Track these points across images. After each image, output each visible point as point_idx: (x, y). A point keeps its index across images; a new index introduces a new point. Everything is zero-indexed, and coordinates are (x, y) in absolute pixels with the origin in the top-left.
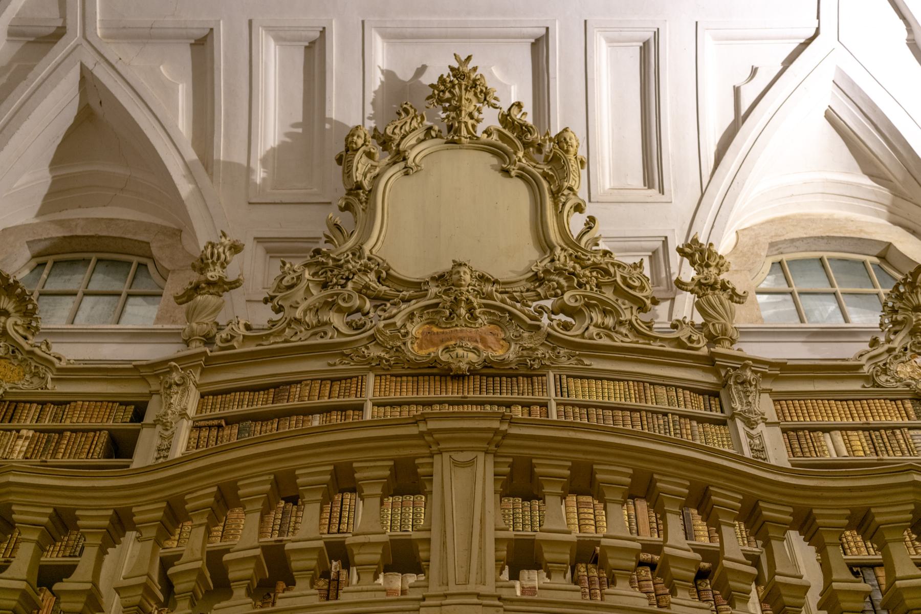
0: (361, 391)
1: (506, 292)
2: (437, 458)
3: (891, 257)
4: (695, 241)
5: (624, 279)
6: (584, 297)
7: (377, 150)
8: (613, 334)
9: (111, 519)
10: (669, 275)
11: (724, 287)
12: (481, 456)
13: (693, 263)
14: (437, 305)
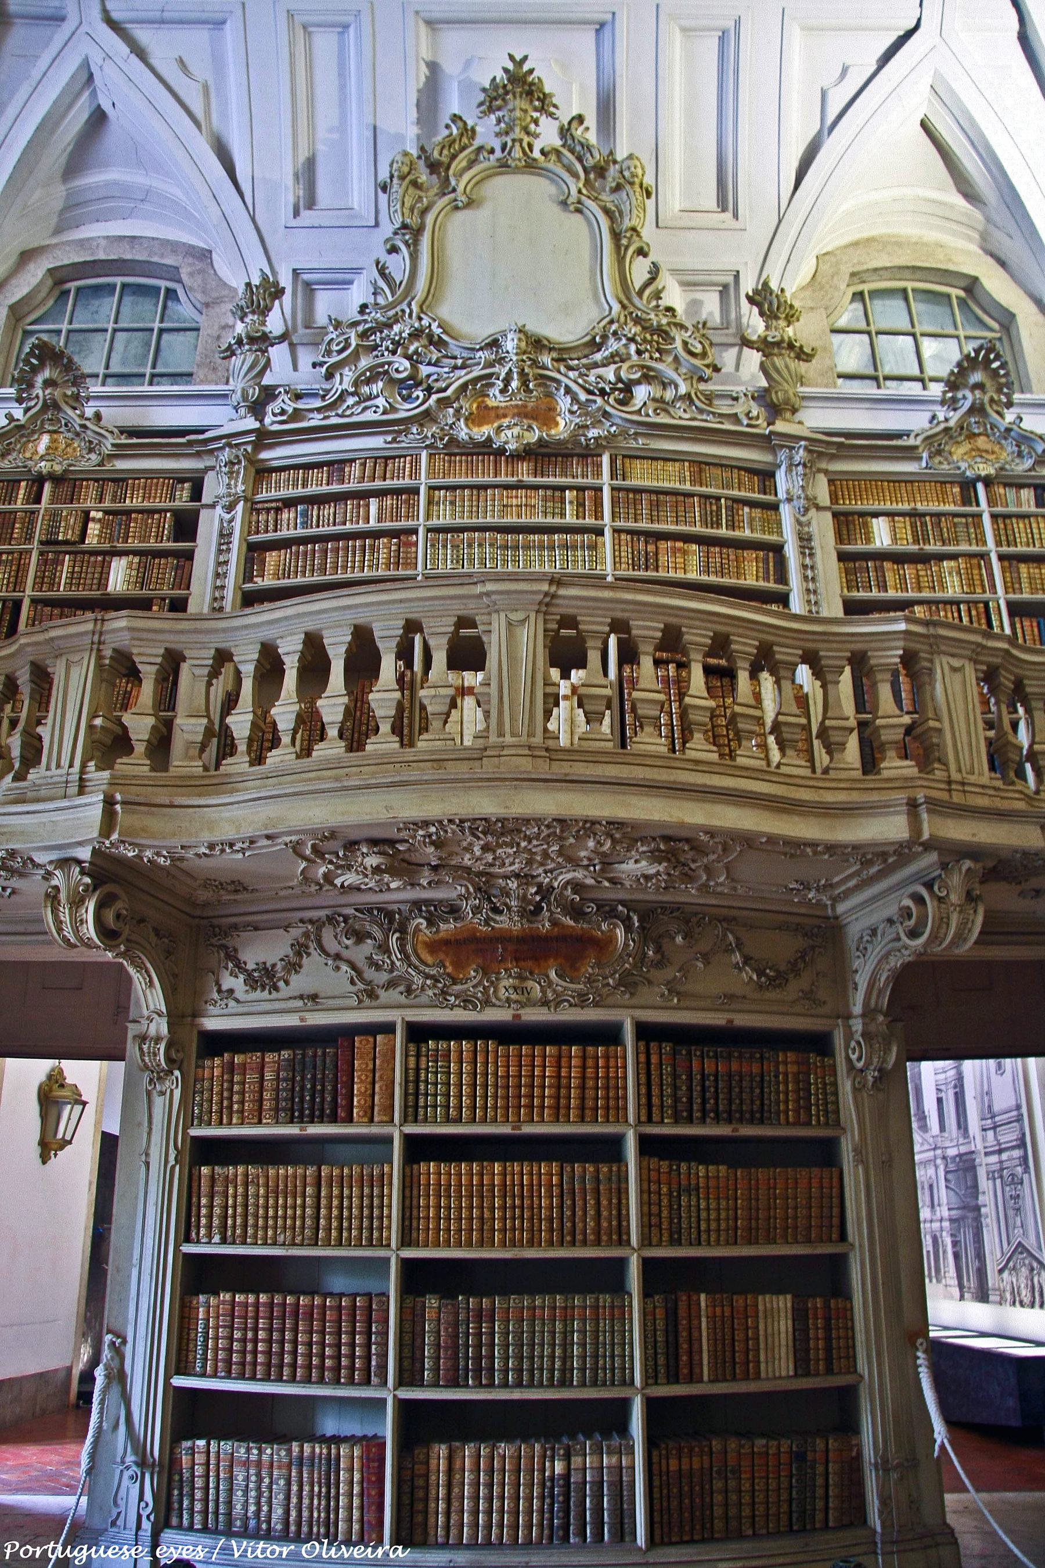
0: (415, 473)
1: (564, 360)
2: (495, 616)
3: (977, 291)
4: (766, 284)
5: (685, 343)
6: (643, 367)
7: (424, 177)
8: (671, 410)
9: (214, 658)
10: (739, 317)
11: (791, 346)
12: (533, 616)
13: (762, 314)
14: (490, 376)
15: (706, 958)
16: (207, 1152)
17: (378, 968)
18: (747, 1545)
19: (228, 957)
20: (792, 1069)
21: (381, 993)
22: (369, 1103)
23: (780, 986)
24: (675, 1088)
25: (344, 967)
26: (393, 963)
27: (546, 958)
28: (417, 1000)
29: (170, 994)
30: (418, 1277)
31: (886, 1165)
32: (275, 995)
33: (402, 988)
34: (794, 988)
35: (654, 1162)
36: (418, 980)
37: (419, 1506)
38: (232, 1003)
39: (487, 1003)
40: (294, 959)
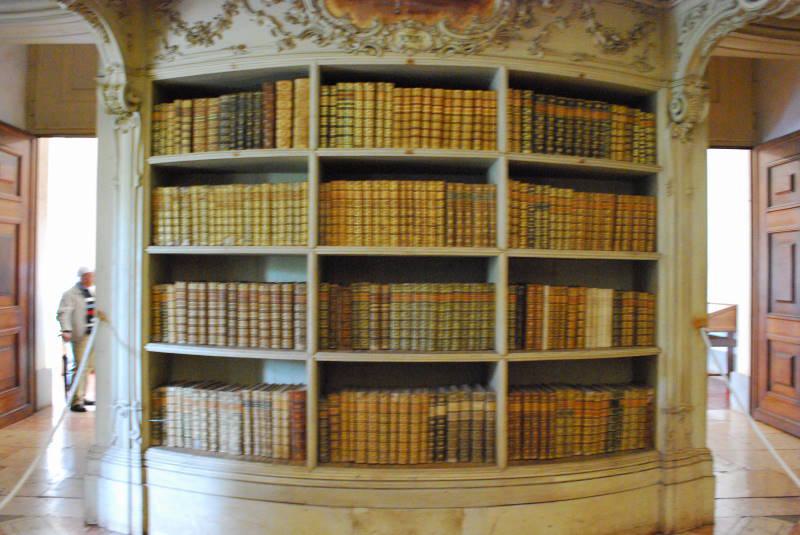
15: (566, 20)
16: (166, 176)
17: (294, 20)
18: (575, 465)
19: (173, 19)
20: (623, 119)
21: (296, 41)
22: (289, 135)
23: (621, 50)
24: (534, 127)
25: (268, 22)
26: (307, 17)
27: (436, 13)
28: (329, 47)
29: (127, 48)
30: (333, 270)
31: (690, 196)
32: (211, 48)
33: (314, 38)
34: (633, 52)
35: (516, 185)
36: (328, 30)
37: (334, 437)
38: (177, 57)
39: (386, 49)
40: (225, 16)
